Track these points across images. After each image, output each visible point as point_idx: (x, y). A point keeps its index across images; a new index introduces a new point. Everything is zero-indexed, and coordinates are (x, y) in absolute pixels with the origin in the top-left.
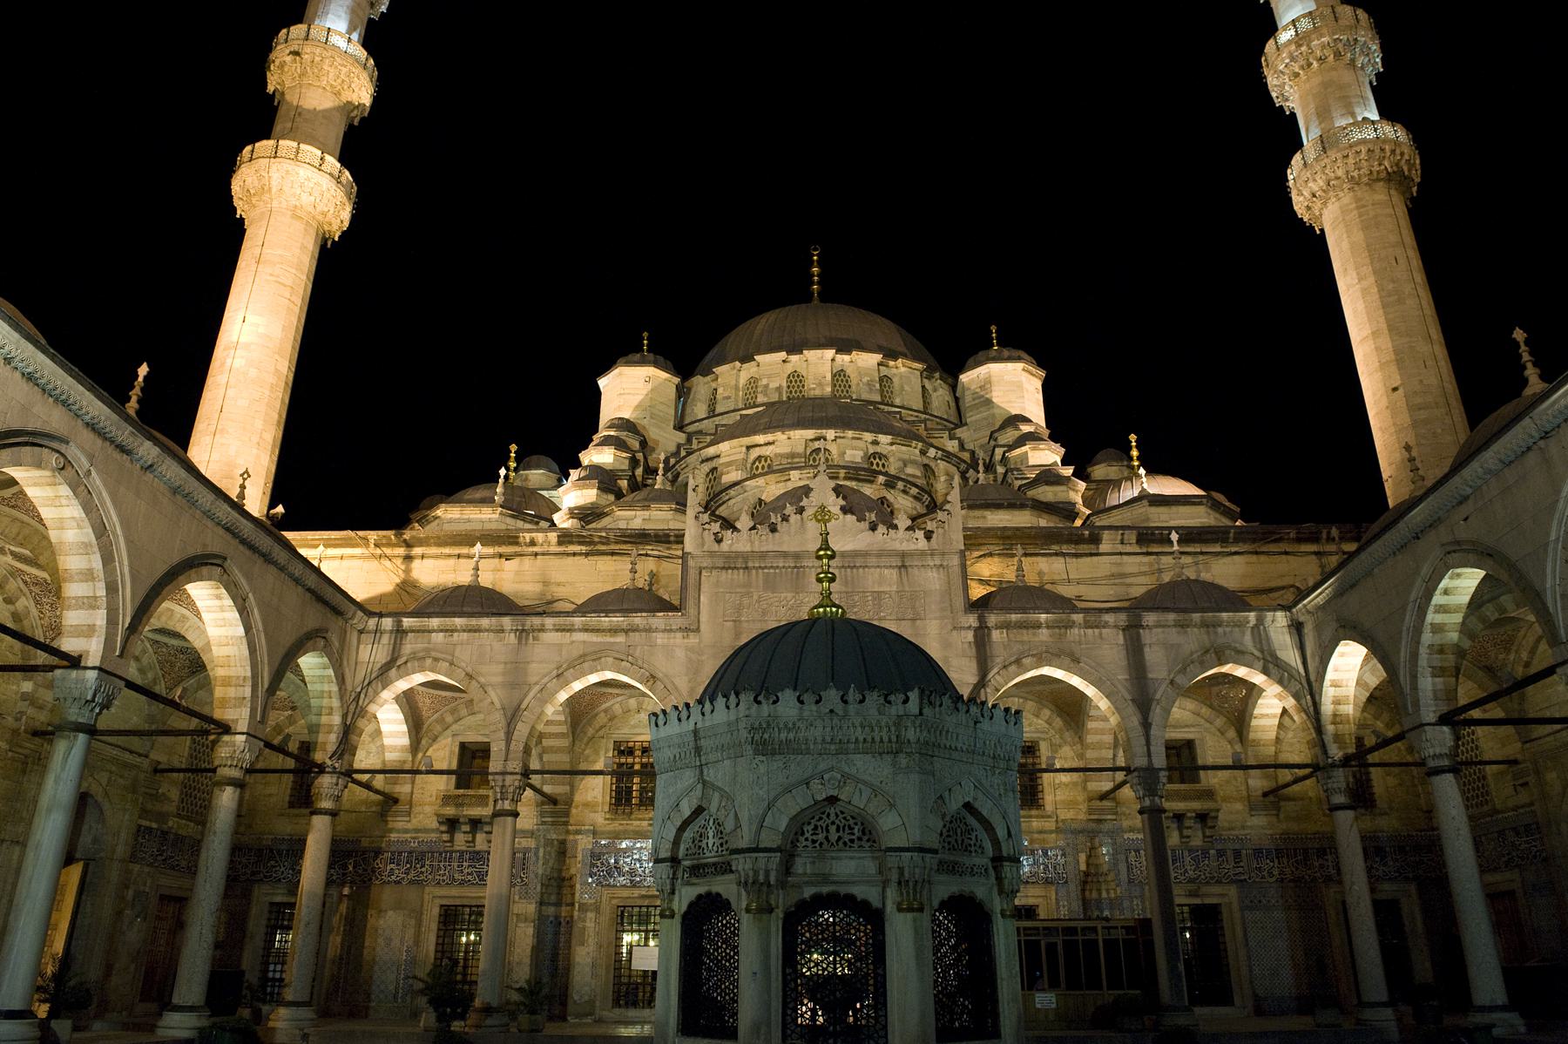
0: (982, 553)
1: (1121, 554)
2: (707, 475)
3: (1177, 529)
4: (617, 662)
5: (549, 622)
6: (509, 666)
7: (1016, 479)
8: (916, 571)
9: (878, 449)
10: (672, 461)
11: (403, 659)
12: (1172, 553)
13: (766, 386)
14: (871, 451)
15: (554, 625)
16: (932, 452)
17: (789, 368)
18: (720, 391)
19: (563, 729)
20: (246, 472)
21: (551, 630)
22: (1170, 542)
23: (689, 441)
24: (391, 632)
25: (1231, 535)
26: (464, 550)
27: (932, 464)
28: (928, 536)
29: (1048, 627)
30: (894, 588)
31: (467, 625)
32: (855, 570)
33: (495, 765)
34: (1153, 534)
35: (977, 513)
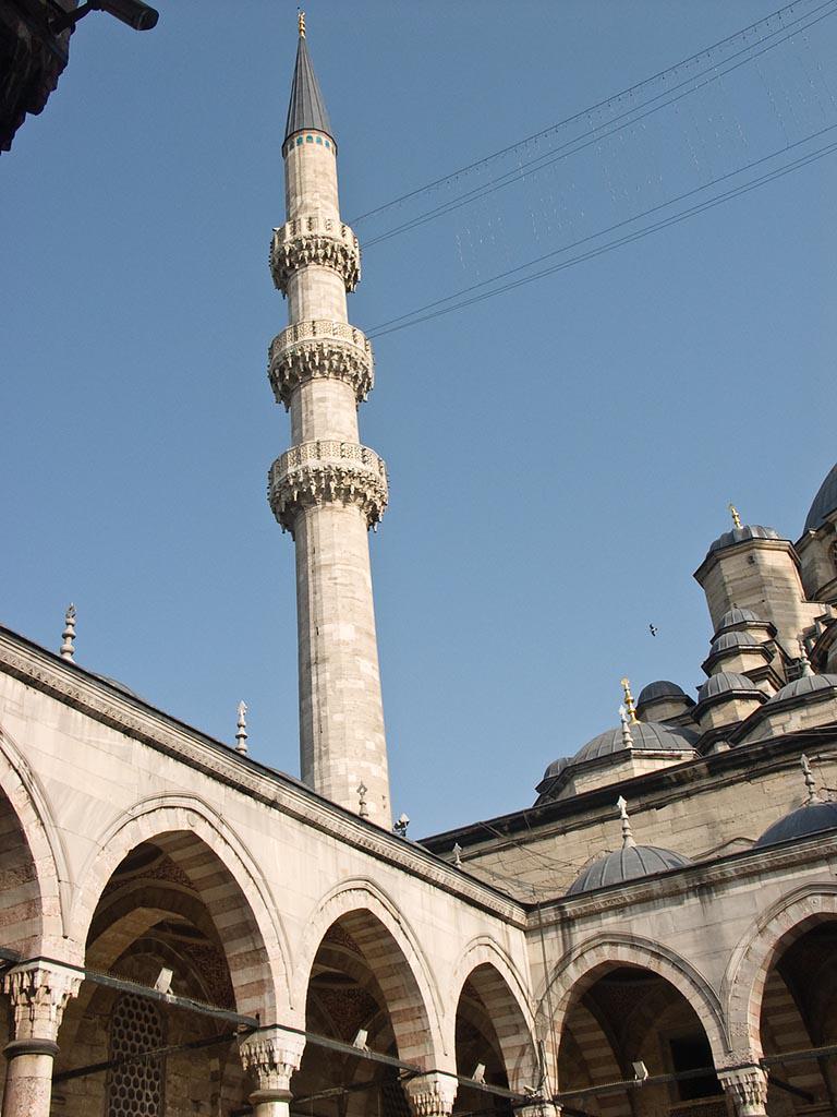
4: (827, 898)
6: (698, 932)
11: (578, 952)
19: (789, 999)
20: (362, 786)
26: (608, 812)
33: (719, 1060)
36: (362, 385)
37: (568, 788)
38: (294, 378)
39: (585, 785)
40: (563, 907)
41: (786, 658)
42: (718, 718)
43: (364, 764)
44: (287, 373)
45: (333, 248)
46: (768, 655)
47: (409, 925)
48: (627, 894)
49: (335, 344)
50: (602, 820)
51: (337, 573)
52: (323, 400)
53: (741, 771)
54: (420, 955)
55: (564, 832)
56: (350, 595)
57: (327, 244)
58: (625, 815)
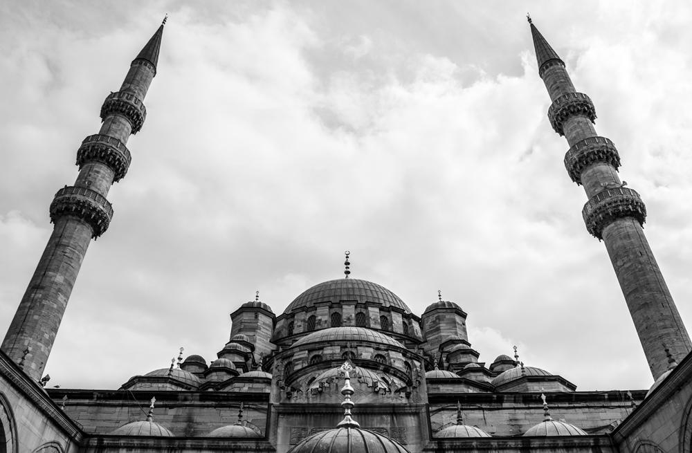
0: (438, 408)
1: (515, 408)
2: (286, 366)
3: (545, 393)
5: (189, 443)
7: (455, 369)
8: (402, 417)
9: (380, 352)
10: (267, 359)
12: (542, 408)
13: (320, 320)
14: (376, 353)
15: (191, 445)
16: (409, 355)
17: (333, 311)
18: (295, 322)
21: (188, 449)
22: (542, 402)
23: (278, 349)
24: (96, 447)
25: (574, 397)
26: (147, 403)
27: (409, 362)
28: (408, 396)
29: (478, 449)
30: (389, 426)
31: (140, 444)
32: (366, 416)
34: (531, 397)
35: (434, 386)
36: (119, 174)
37: (133, 387)
38: (88, 157)
39: (139, 387)
40: (103, 440)
41: (254, 362)
42: (214, 377)
43: (39, 344)
44: (86, 153)
45: (133, 112)
46: (247, 358)
47: (15, 424)
48: (136, 442)
49: (115, 151)
50: (143, 406)
51: (68, 251)
52: (98, 172)
53: (214, 403)
54: (15, 441)
55: (122, 406)
56: (69, 262)
57: (132, 109)
58: (152, 406)
